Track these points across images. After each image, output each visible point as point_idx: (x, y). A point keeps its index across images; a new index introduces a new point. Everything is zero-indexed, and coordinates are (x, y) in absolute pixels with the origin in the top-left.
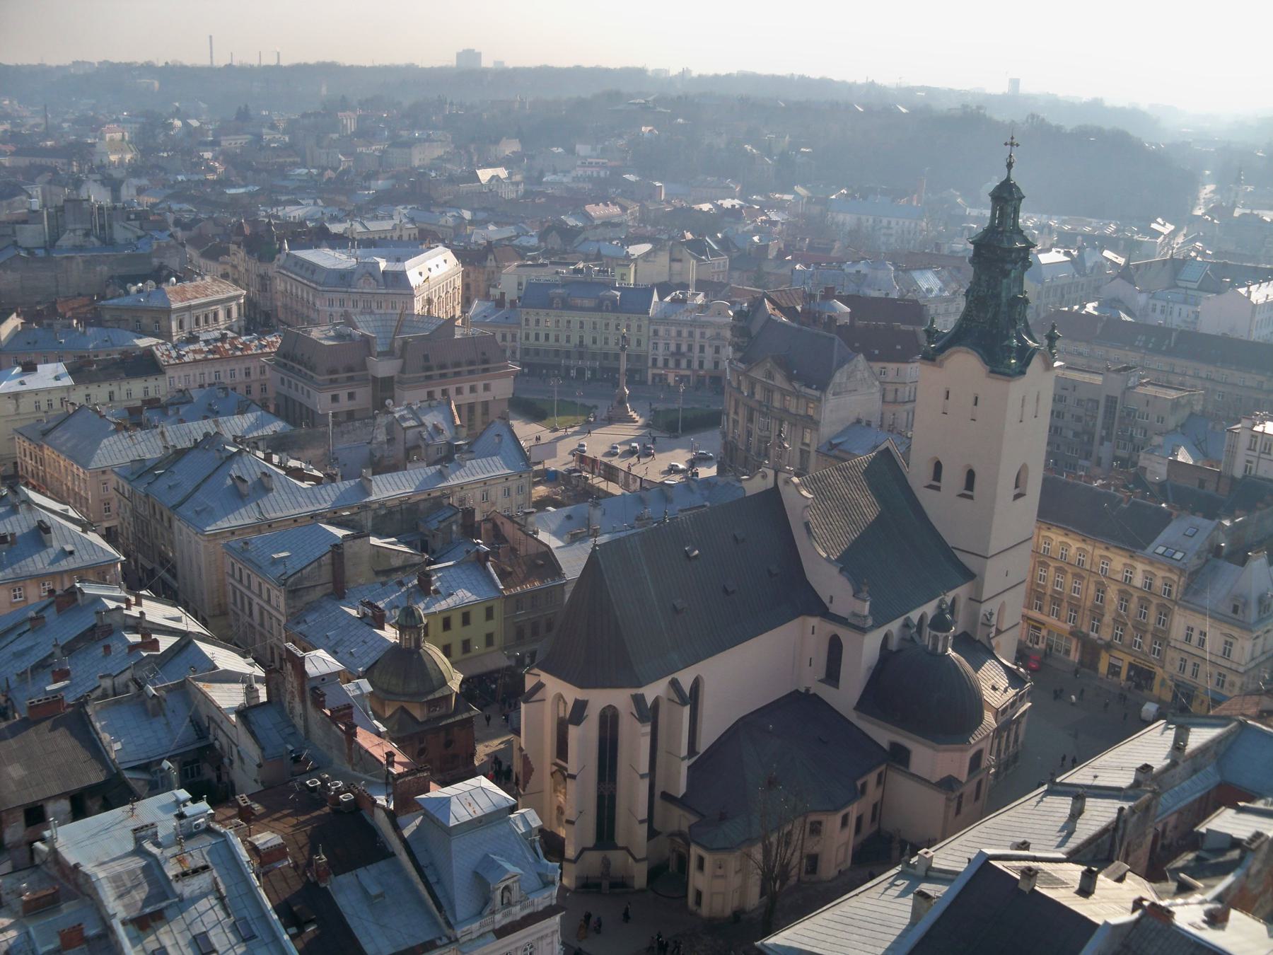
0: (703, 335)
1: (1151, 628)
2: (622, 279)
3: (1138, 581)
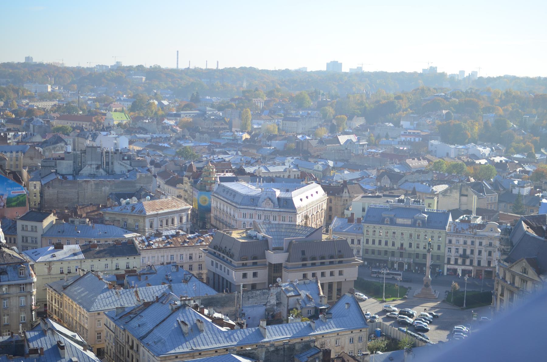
0: (481, 244)
2: (429, 206)
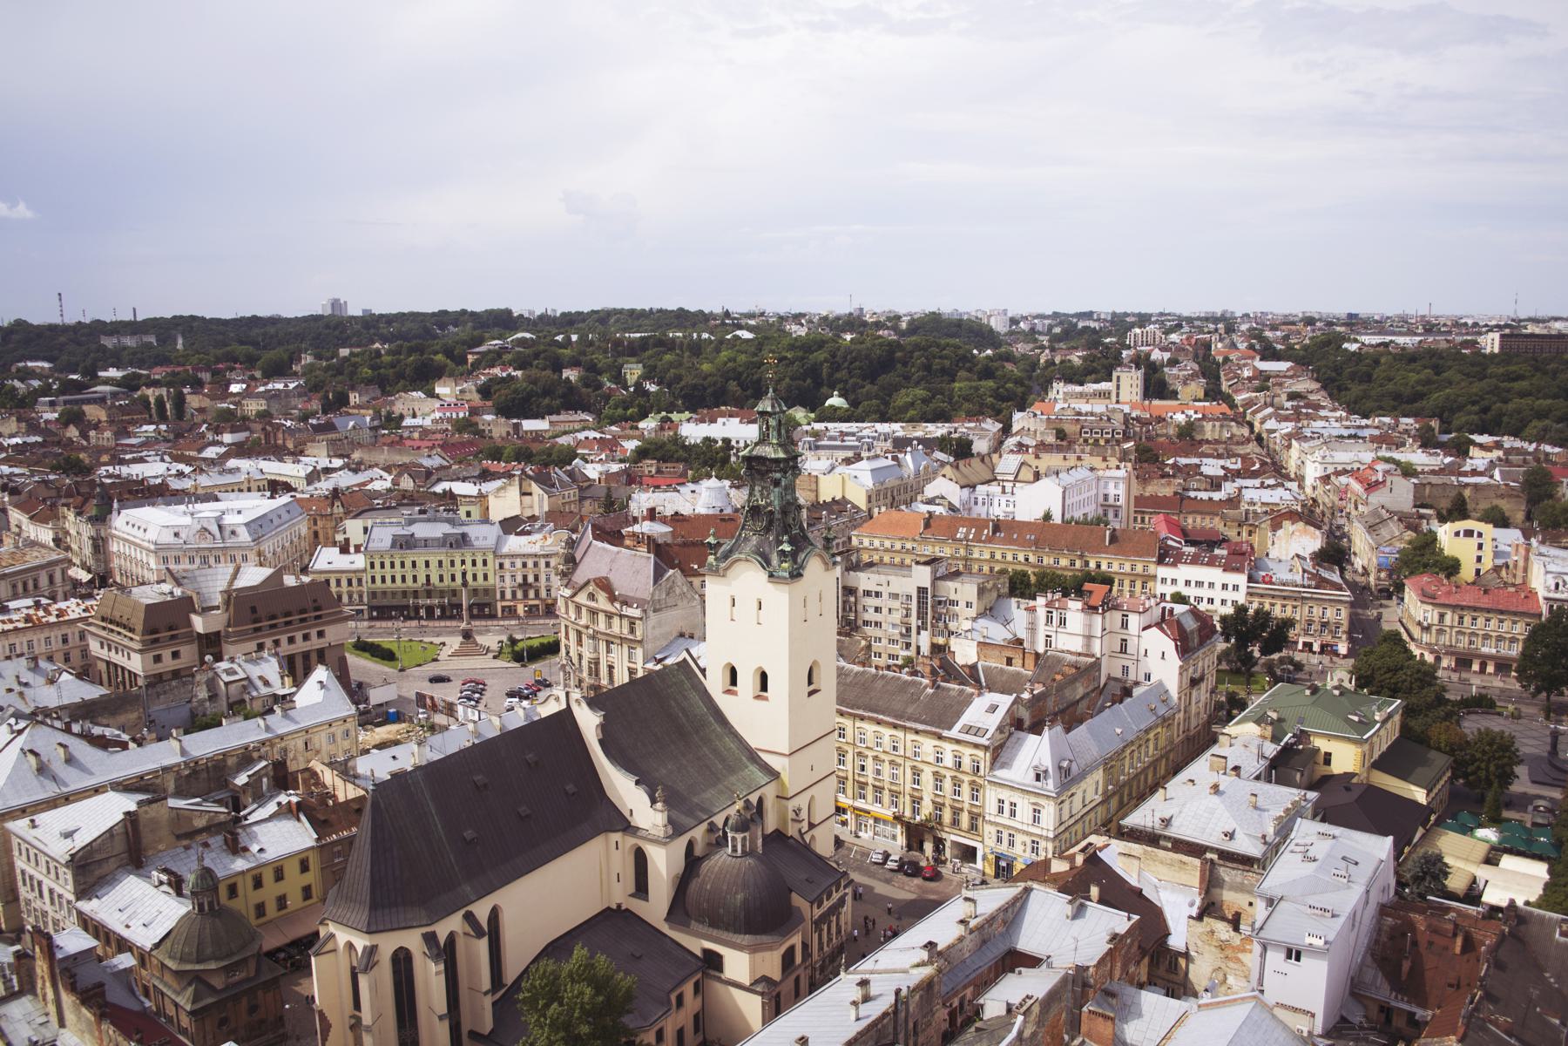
0: (548, 565)
1: (966, 806)
3: (949, 761)
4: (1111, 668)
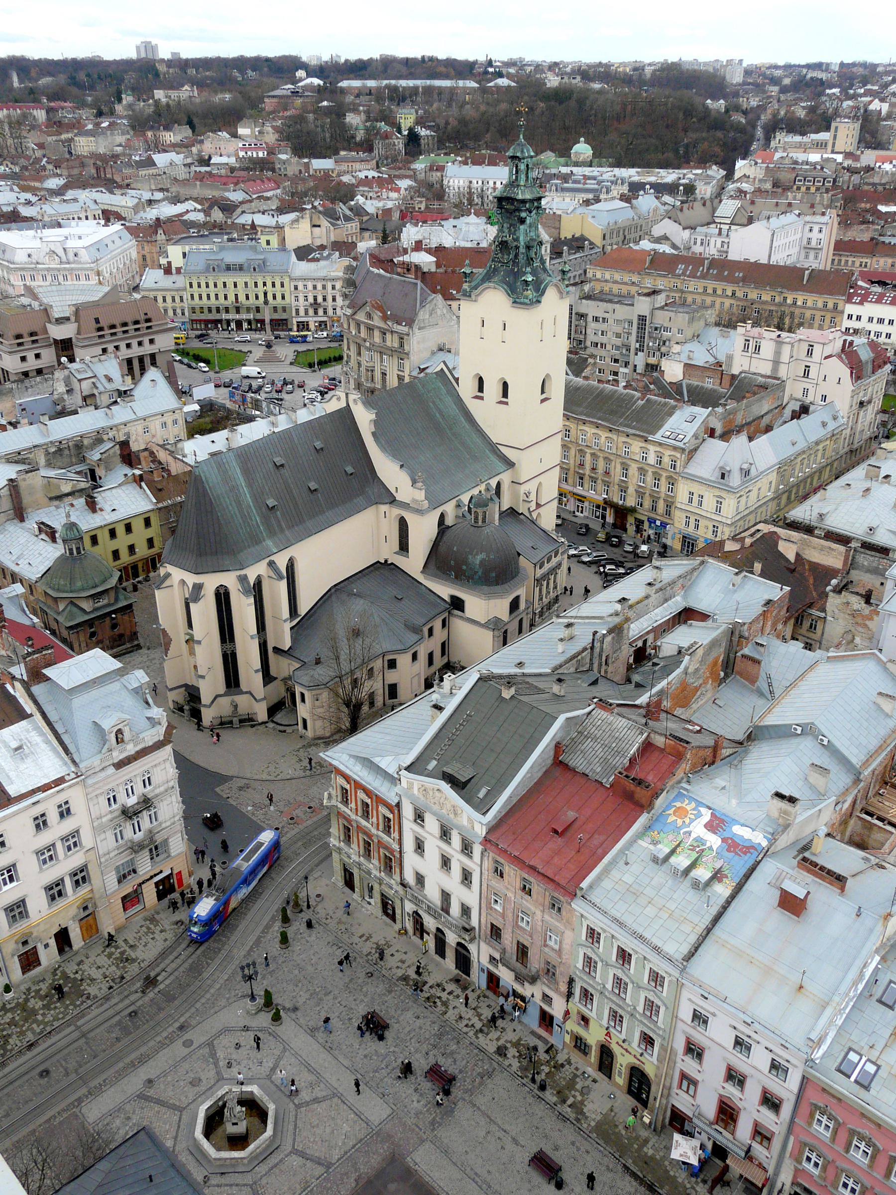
0: (333, 288)
1: (663, 495)
3: (652, 459)
4: (794, 390)
